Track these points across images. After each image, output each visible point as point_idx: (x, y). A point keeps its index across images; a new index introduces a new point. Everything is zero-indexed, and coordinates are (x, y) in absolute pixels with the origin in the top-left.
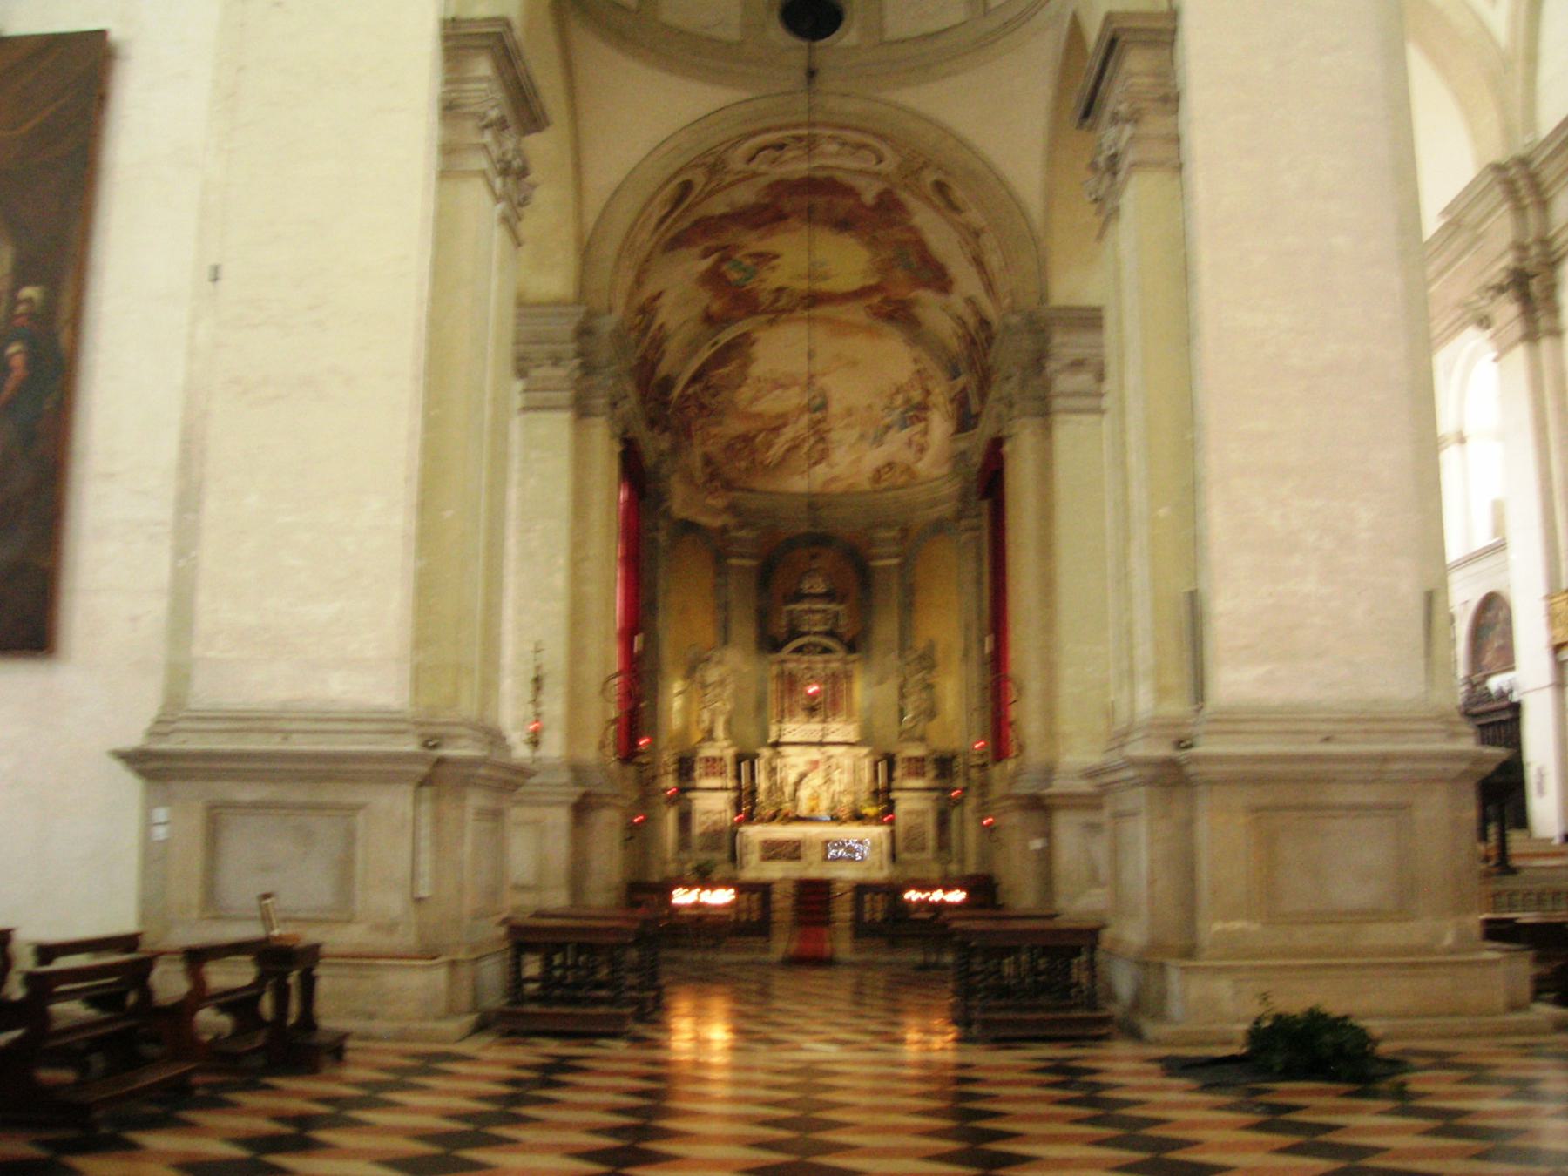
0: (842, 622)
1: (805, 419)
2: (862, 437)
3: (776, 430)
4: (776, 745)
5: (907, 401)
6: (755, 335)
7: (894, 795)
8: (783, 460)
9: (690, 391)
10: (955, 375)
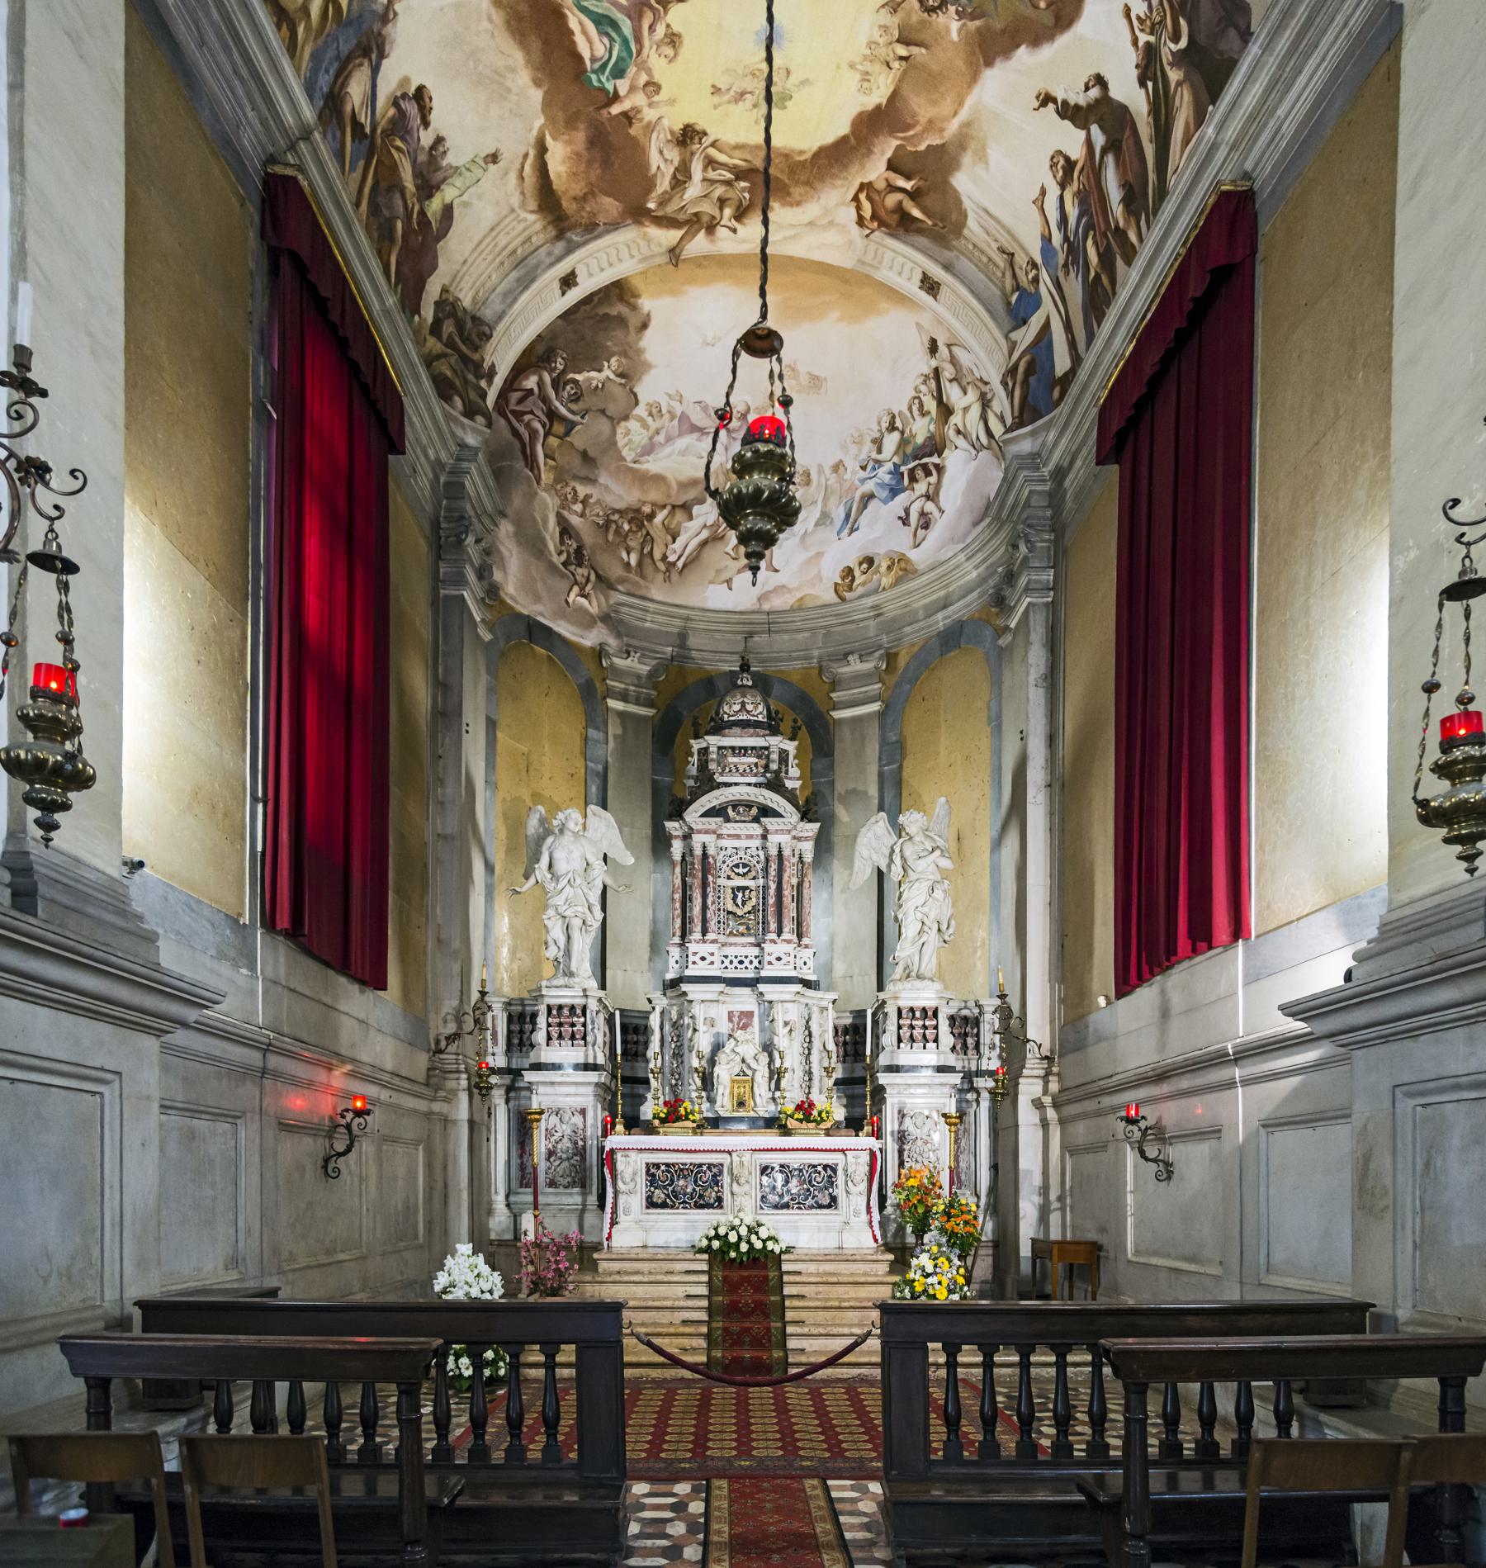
0: (794, 772)
4: (675, 983)
7: (883, 1079)
10: (1018, 314)
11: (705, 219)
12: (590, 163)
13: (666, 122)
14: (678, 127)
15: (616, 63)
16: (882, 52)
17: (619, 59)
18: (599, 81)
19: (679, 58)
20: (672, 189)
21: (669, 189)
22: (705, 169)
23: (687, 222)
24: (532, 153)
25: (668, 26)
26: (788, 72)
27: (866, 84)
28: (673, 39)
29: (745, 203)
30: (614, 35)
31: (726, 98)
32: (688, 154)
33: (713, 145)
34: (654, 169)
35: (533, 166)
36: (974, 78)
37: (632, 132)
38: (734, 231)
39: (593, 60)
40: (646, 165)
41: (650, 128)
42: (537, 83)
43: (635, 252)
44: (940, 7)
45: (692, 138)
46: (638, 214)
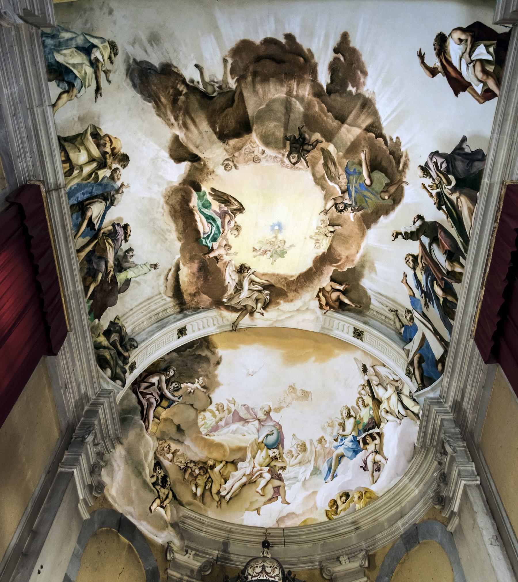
1: (262, 455)
2: (316, 471)
3: (234, 463)
5: (357, 423)
6: (220, 352)
8: (236, 496)
9: (154, 380)
11: (249, 308)
12: (198, 278)
13: (233, 262)
14: (238, 265)
15: (213, 236)
16: (323, 230)
17: (215, 234)
18: (206, 242)
19: (240, 236)
20: (235, 293)
21: (233, 293)
22: (250, 284)
23: (240, 310)
24: (173, 269)
25: (236, 222)
26: (285, 242)
27: (317, 245)
28: (237, 228)
29: (268, 301)
30: (213, 224)
31: (259, 253)
32: (242, 277)
33: (253, 273)
34: (227, 283)
35: (173, 275)
36: (363, 234)
37: (218, 265)
38: (263, 314)
39: (204, 233)
40: (223, 281)
41: (226, 264)
42: (179, 239)
43: (215, 322)
44: (344, 209)
45: (244, 270)
46: (218, 303)
